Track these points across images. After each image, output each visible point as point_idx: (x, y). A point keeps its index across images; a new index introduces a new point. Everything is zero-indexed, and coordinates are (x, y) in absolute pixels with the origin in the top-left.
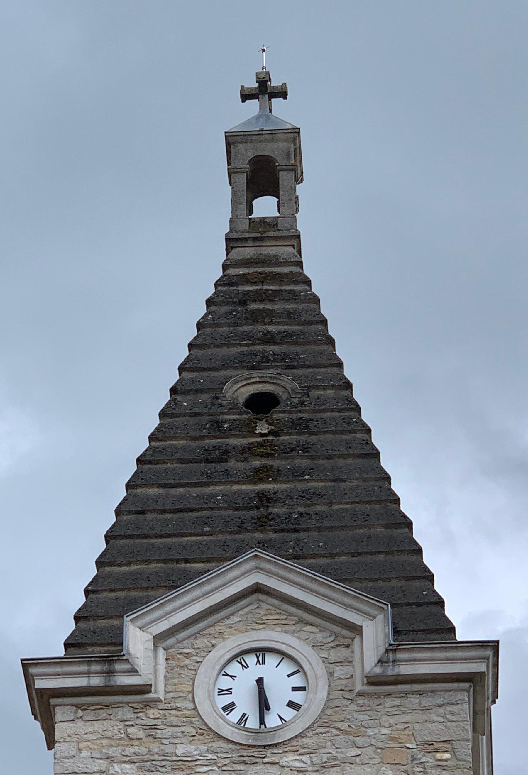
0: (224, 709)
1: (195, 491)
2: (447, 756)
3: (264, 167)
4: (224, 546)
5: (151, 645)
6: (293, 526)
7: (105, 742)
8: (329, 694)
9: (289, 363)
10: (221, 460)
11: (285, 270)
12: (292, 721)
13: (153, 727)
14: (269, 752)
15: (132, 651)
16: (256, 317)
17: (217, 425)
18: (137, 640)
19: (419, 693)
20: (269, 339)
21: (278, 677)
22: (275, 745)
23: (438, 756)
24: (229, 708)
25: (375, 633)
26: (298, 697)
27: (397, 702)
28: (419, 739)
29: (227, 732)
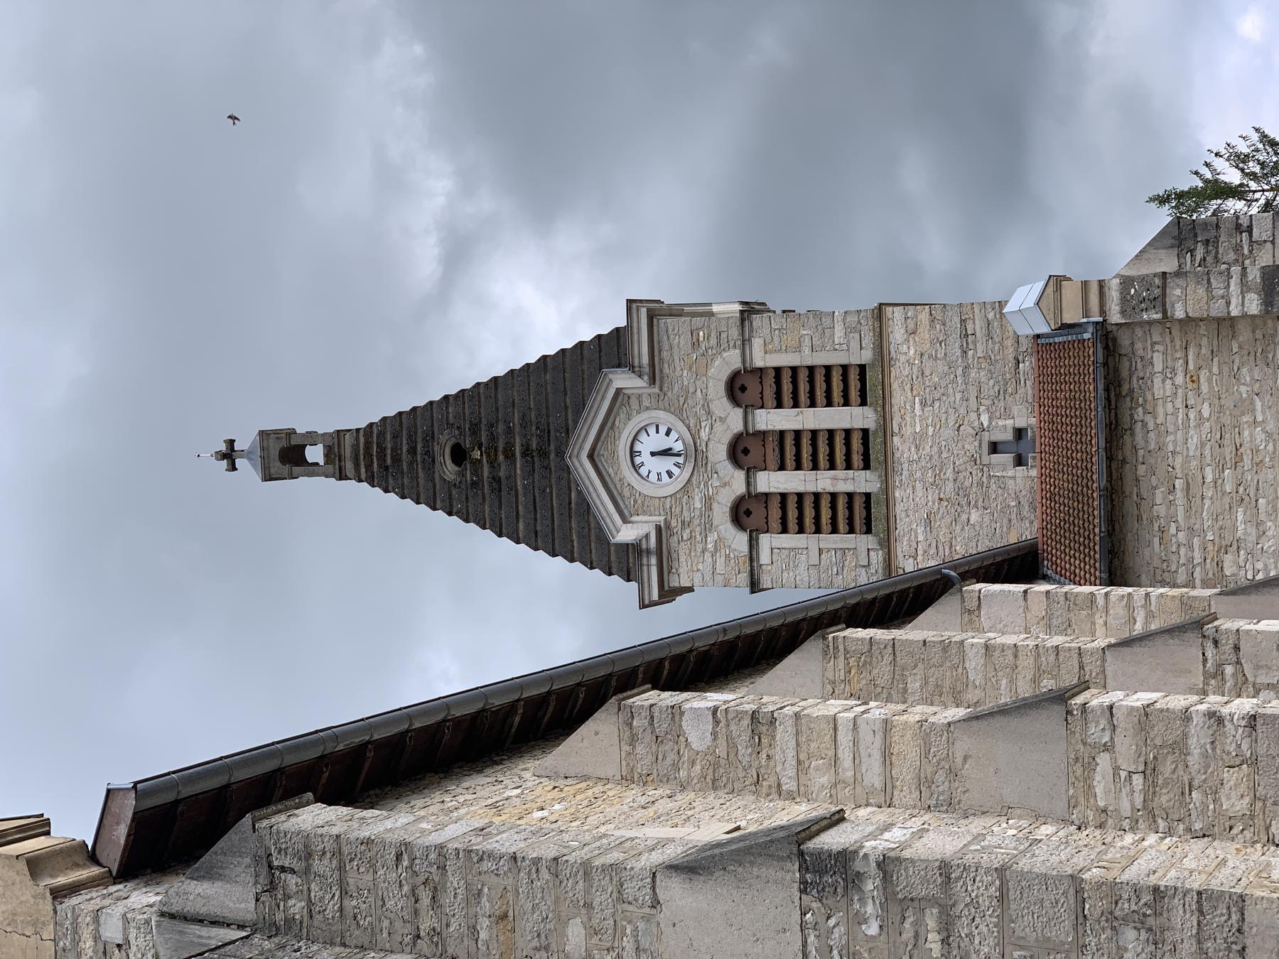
1: (521, 498)
3: (285, 455)
4: (560, 478)
6: (545, 434)
9: (430, 437)
10: (499, 481)
11: (362, 440)
12: (679, 433)
13: (683, 523)
16: (397, 460)
17: (474, 484)
18: (626, 534)
19: (660, 351)
20: (412, 451)
24: (670, 474)
25: (621, 380)
26: (663, 430)
27: (666, 365)
29: (686, 475)
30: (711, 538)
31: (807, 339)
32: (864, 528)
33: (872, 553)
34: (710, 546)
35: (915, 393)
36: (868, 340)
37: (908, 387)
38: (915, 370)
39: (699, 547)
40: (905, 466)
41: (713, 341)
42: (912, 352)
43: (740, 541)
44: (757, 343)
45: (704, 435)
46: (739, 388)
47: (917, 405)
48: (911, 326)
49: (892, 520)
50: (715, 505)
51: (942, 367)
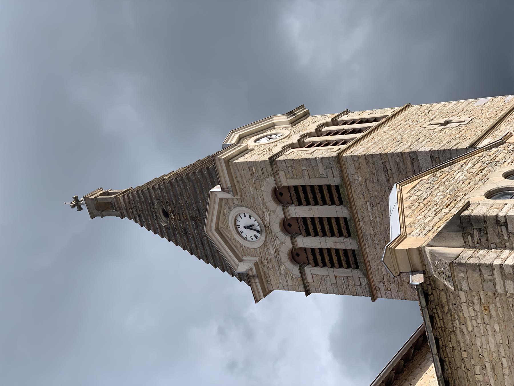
0: (257, 238)
2: (253, 169)
5: (242, 263)
7: (276, 275)
8: (244, 206)
12: (255, 218)
13: (267, 260)
14: (267, 225)
15: (245, 270)
19: (236, 177)
21: (243, 222)
22: (264, 223)
23: (254, 171)
24: (256, 237)
26: (247, 216)
27: (241, 184)
28: (250, 177)
29: (263, 238)
30: (282, 268)
31: (306, 172)
32: (355, 266)
33: (361, 279)
34: (283, 272)
35: (366, 200)
36: (336, 172)
37: (362, 197)
38: (364, 188)
39: (278, 272)
40: (369, 237)
41: (260, 173)
42: (360, 179)
43: (295, 270)
44: (281, 174)
45: (267, 218)
46: (279, 195)
47: (369, 206)
48: (357, 165)
49: (368, 264)
50: (280, 253)
51: (377, 187)
